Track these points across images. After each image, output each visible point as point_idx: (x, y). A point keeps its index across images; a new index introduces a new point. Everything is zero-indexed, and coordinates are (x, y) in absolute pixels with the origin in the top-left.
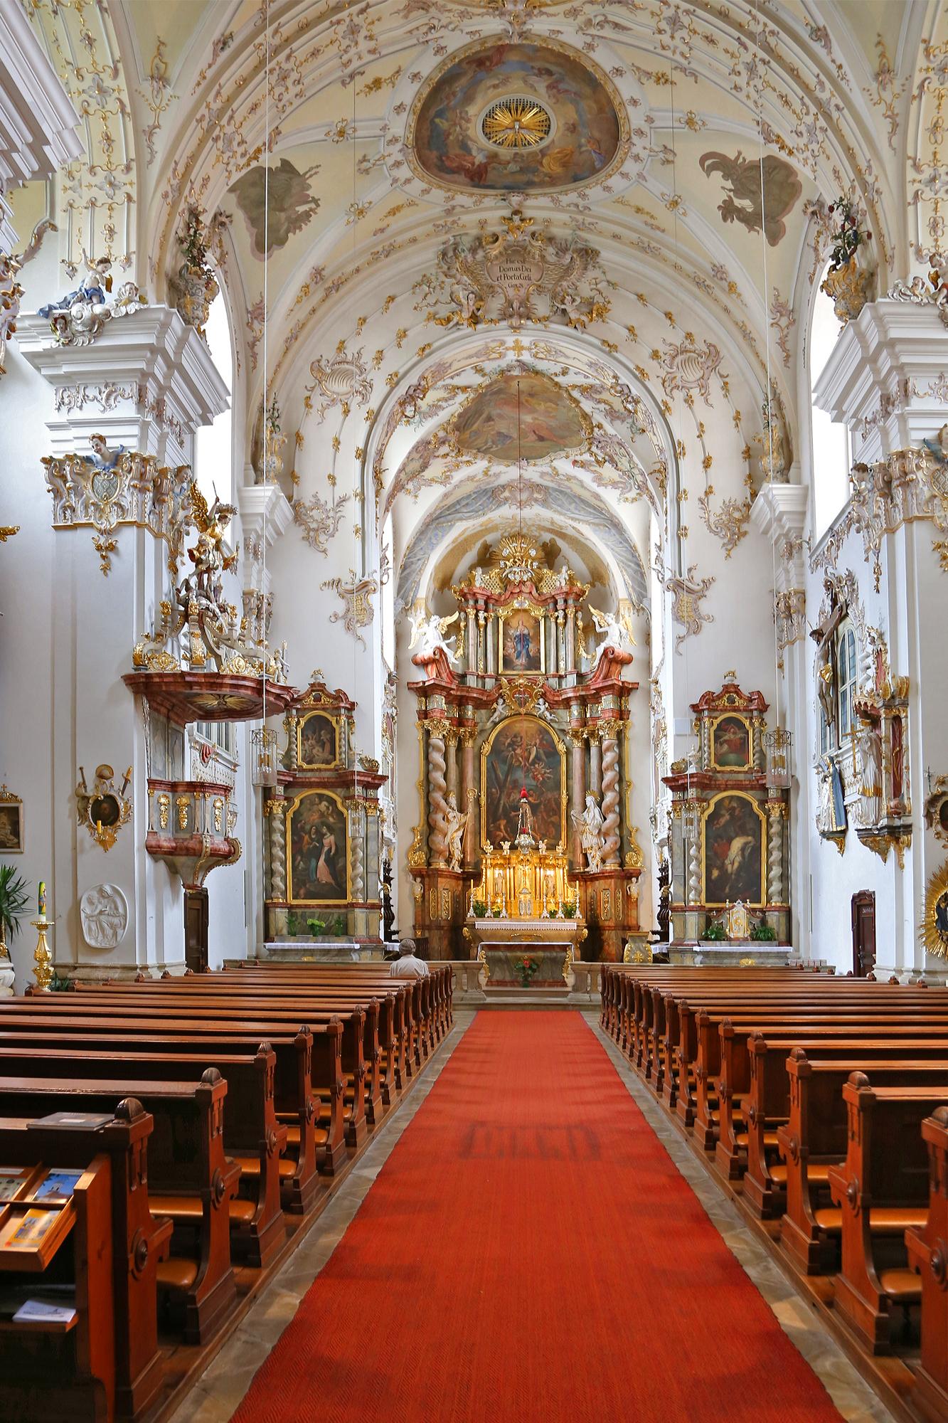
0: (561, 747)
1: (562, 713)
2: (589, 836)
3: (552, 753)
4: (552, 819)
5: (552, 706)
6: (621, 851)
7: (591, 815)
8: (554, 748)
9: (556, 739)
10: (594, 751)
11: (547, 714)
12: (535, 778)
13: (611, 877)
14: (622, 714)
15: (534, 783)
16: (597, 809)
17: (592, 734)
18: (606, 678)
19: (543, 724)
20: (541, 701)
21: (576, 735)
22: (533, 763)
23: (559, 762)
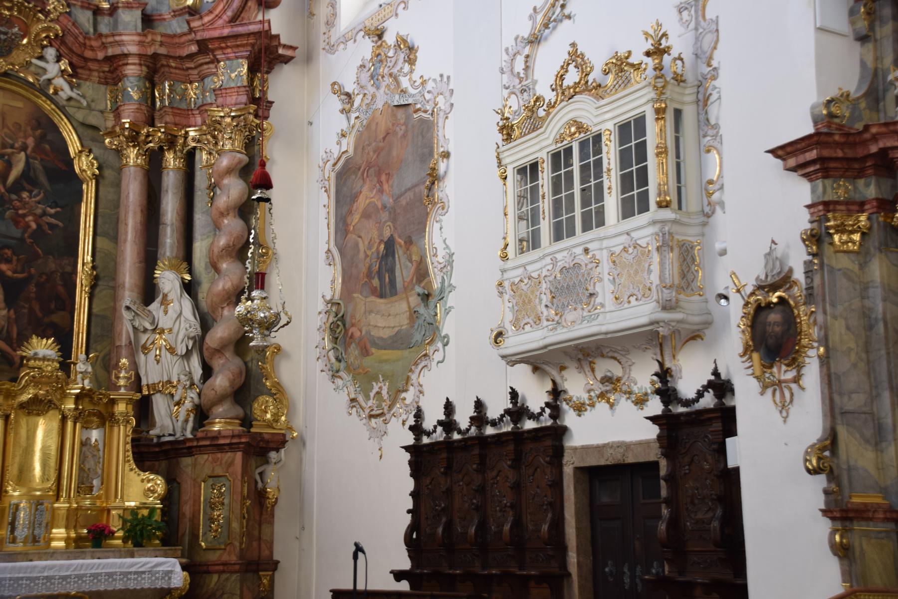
0: (84, 165)
1: (92, 89)
2: (166, 356)
3: (63, 181)
4: (56, 318)
5: (75, 74)
6: (244, 392)
7: (173, 308)
8: (70, 162)
9: (74, 144)
10: (171, 180)
11: (60, 82)
12: (17, 220)
13: (232, 447)
14: (260, 104)
15: (16, 232)
16: (187, 303)
17: (171, 142)
18: (233, 20)
19: (48, 106)
20: (50, 53)
21: (134, 138)
22: (17, 187)
23: (78, 197)
